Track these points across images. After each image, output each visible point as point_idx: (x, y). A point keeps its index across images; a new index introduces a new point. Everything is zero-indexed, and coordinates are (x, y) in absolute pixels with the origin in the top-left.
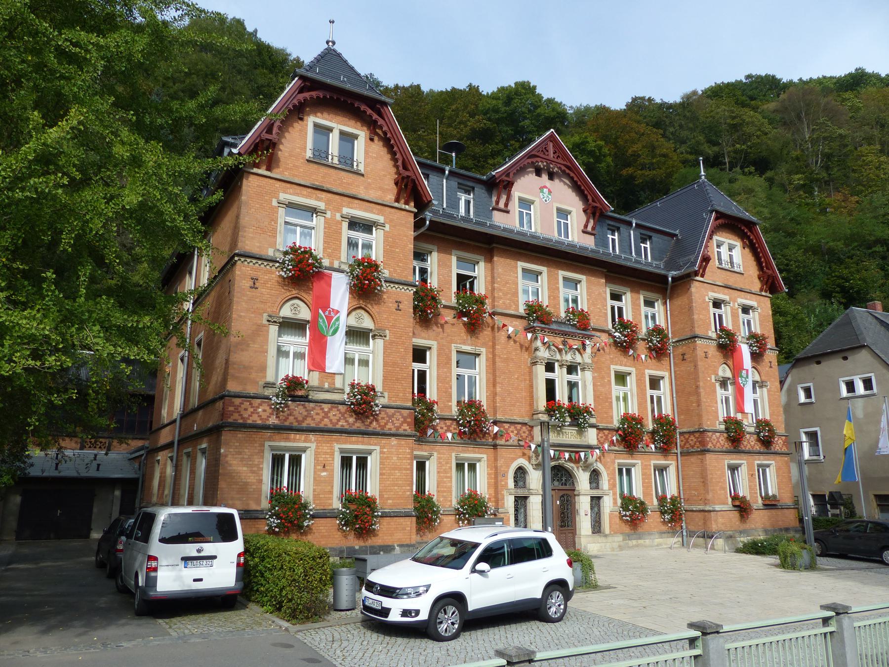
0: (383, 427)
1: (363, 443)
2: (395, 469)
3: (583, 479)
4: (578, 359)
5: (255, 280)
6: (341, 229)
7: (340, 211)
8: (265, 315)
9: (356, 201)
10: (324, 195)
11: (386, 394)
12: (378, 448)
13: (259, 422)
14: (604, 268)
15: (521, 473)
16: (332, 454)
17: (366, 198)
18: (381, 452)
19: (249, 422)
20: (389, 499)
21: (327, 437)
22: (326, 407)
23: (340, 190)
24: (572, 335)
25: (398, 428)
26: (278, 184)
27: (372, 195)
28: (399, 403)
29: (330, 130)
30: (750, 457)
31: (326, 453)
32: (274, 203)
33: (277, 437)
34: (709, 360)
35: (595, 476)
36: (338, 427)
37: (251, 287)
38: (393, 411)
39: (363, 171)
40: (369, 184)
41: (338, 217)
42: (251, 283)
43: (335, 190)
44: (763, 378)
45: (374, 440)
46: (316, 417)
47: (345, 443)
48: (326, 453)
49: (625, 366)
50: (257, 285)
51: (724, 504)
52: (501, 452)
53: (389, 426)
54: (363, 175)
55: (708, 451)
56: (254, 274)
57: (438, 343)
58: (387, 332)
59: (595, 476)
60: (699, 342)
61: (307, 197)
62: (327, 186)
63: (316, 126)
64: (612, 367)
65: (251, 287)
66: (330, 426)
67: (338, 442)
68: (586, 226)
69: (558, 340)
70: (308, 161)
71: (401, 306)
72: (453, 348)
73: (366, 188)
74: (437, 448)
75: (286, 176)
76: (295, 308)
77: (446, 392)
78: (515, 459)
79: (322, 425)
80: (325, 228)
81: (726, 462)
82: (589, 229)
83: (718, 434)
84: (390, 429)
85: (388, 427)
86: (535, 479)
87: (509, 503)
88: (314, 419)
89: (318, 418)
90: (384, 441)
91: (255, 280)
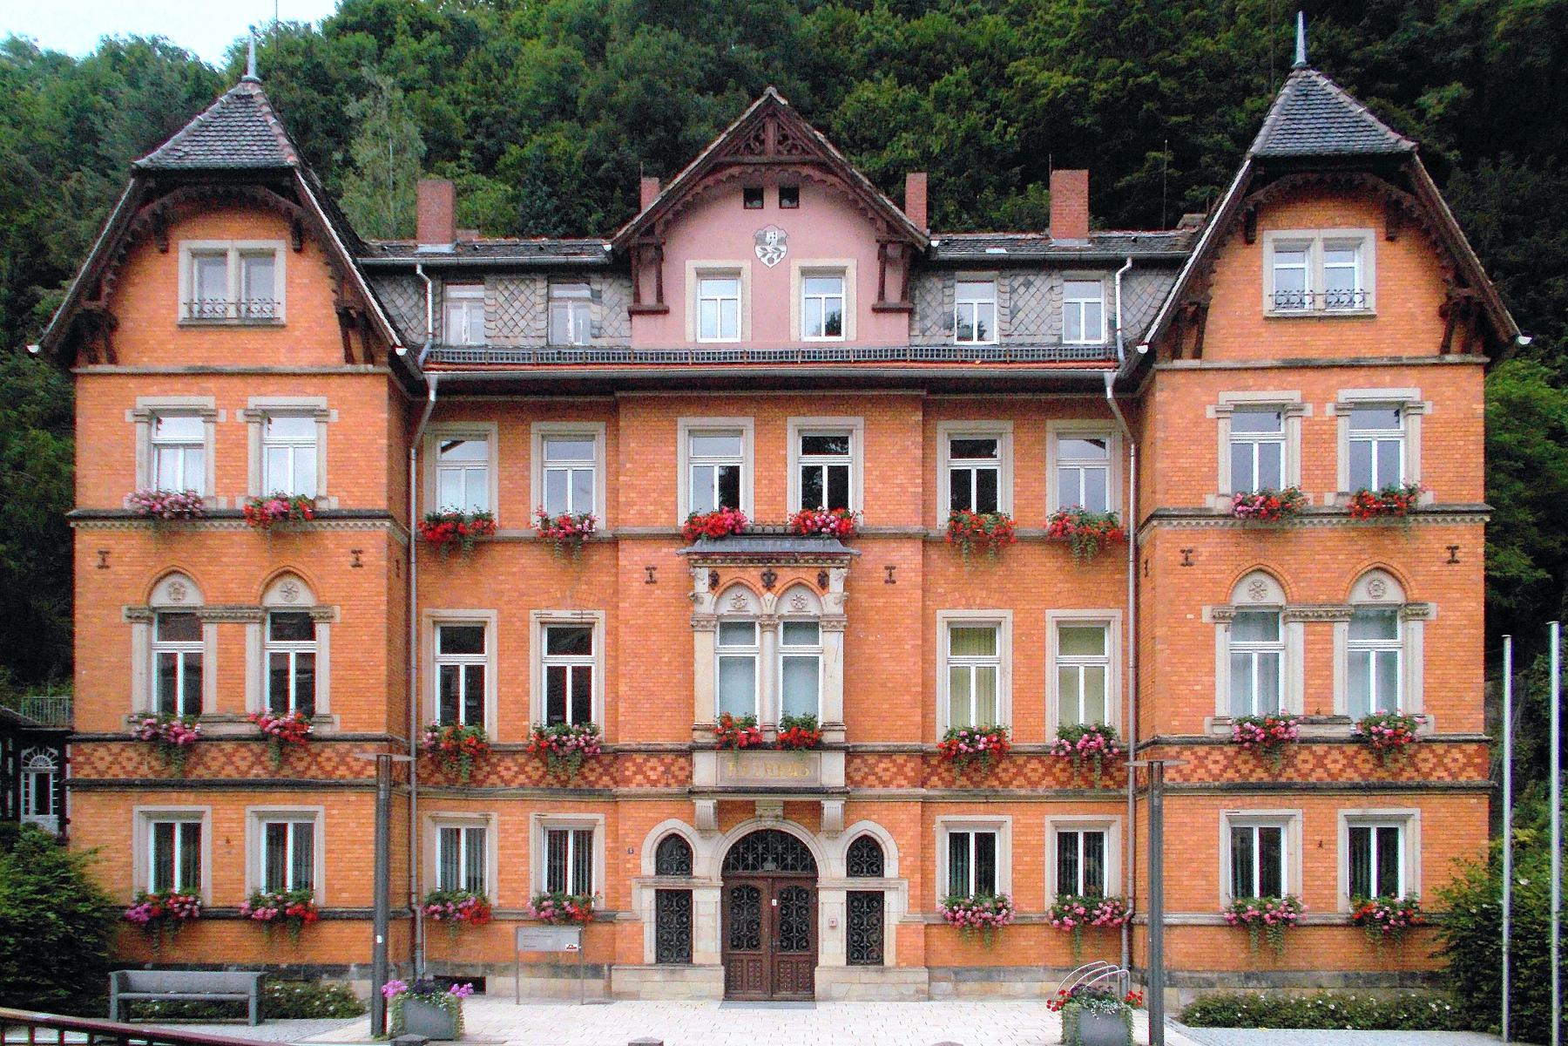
0: (329, 774)
1: (294, 802)
2: (354, 842)
3: (831, 862)
4: (812, 609)
5: (104, 554)
6: (246, 438)
7: (242, 402)
8: (124, 610)
9: (272, 380)
10: (211, 384)
11: (337, 718)
12: (320, 809)
13: (122, 777)
14: (922, 388)
15: (674, 853)
16: (242, 821)
17: (290, 368)
18: (328, 816)
19: (108, 777)
20: (341, 890)
21: (230, 795)
22: (228, 747)
23: (243, 365)
24: (792, 558)
25: (358, 774)
26: (132, 384)
27: (303, 362)
28: (361, 731)
29: (223, 254)
30: (1320, 804)
31: (232, 820)
32: (129, 418)
33: (151, 797)
34: (1197, 571)
35: (865, 856)
36: (250, 777)
37: (100, 567)
38: (347, 746)
39: (284, 320)
40: (298, 341)
41: (240, 416)
42: (99, 561)
43: (229, 369)
44: (1416, 594)
45: (312, 796)
46: (215, 764)
47: (263, 803)
48: (232, 820)
49: (982, 606)
50: (110, 561)
51: (1200, 910)
52: (626, 809)
53: (342, 770)
54: (283, 326)
55: (1166, 790)
56: (103, 544)
57: (500, 611)
58: (337, 609)
59: (865, 856)
60: (1164, 529)
61: (181, 393)
62: (217, 365)
63: (195, 254)
64: (940, 614)
65: (100, 567)
66: (236, 776)
67: (252, 803)
68: (882, 295)
69: (753, 575)
70: (181, 326)
71: (363, 558)
72: (533, 618)
73: (291, 350)
74: (498, 805)
75: (146, 363)
76: (177, 591)
77: (516, 702)
78: (658, 821)
79: (222, 777)
80: (217, 441)
81: (1223, 814)
82: (893, 297)
83: (1201, 750)
84: (343, 777)
85: (338, 773)
86: (708, 858)
87: (644, 903)
88: (208, 768)
89: (215, 766)
90: (332, 797)
91: (104, 554)
